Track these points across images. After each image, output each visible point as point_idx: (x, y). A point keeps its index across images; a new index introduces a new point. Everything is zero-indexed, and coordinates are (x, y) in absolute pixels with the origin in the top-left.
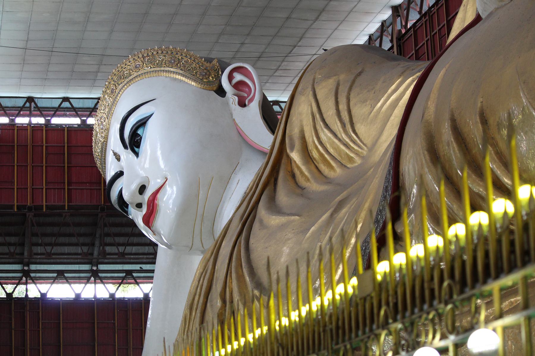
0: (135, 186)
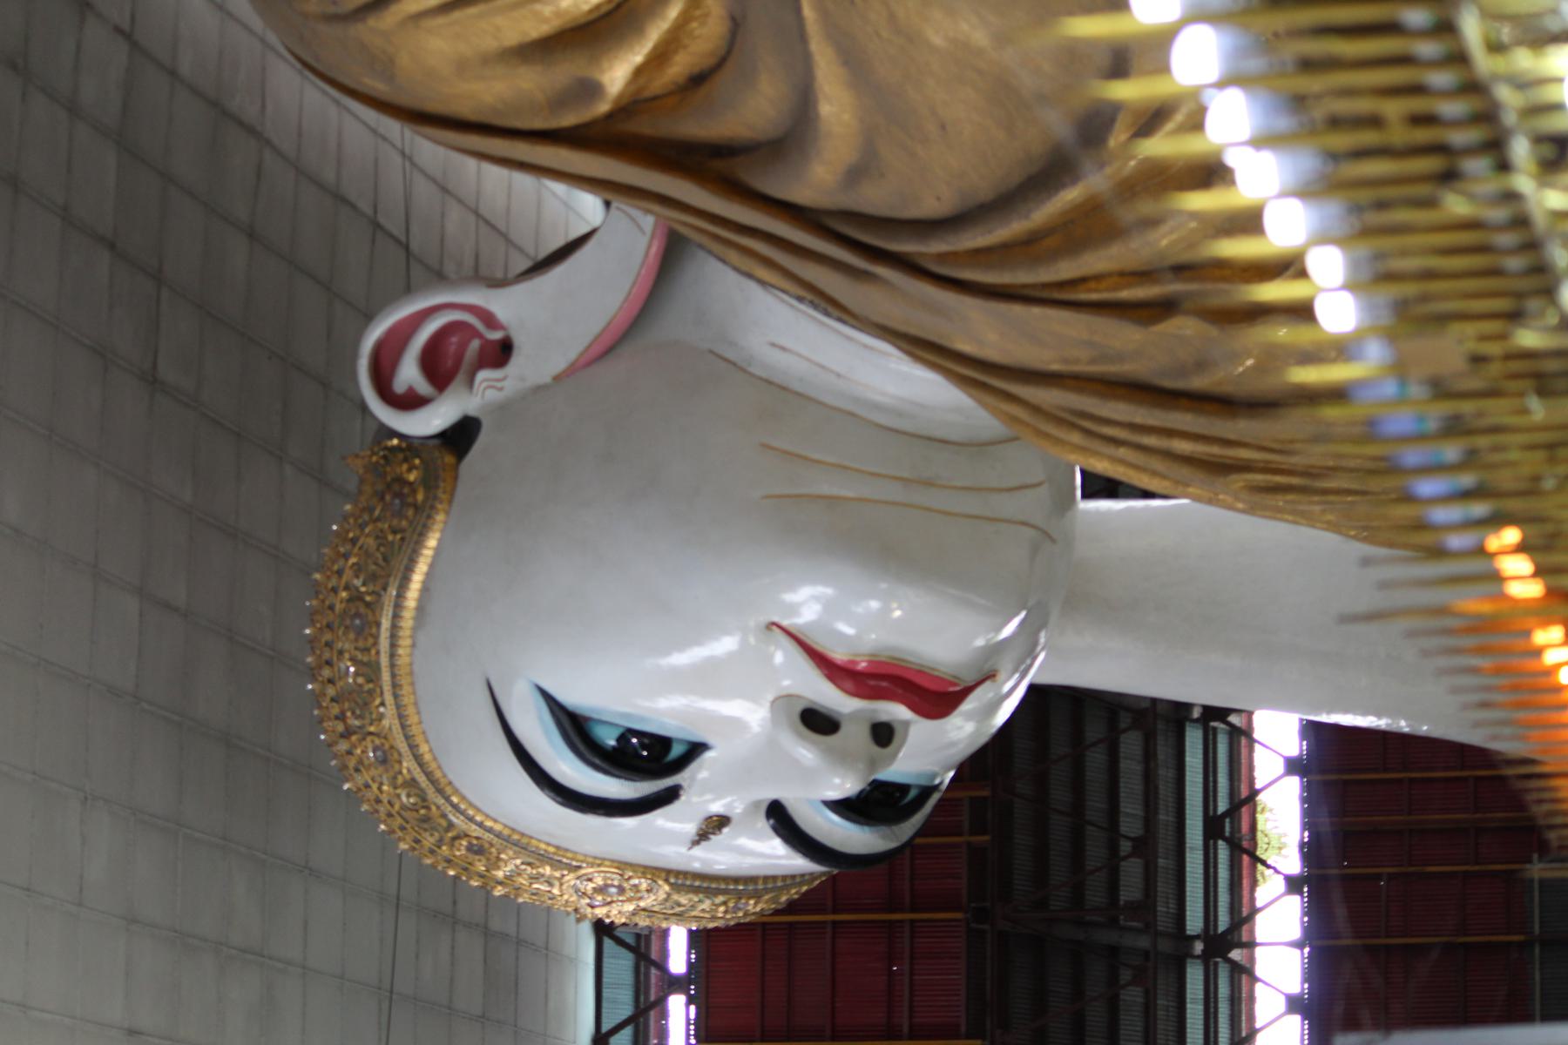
0: (805, 751)
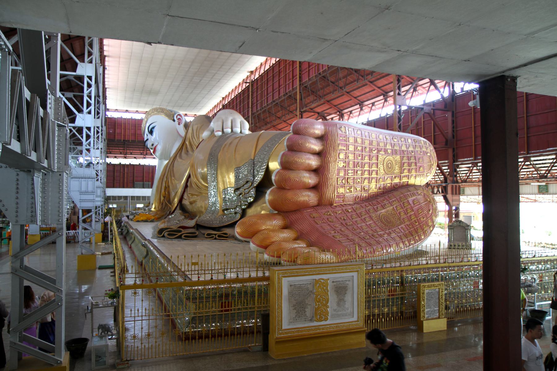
0: (151, 144)
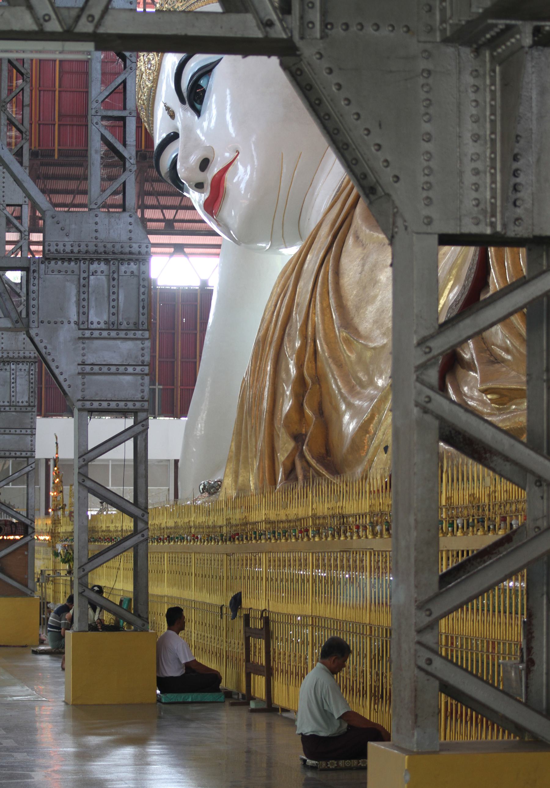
0: (194, 159)
